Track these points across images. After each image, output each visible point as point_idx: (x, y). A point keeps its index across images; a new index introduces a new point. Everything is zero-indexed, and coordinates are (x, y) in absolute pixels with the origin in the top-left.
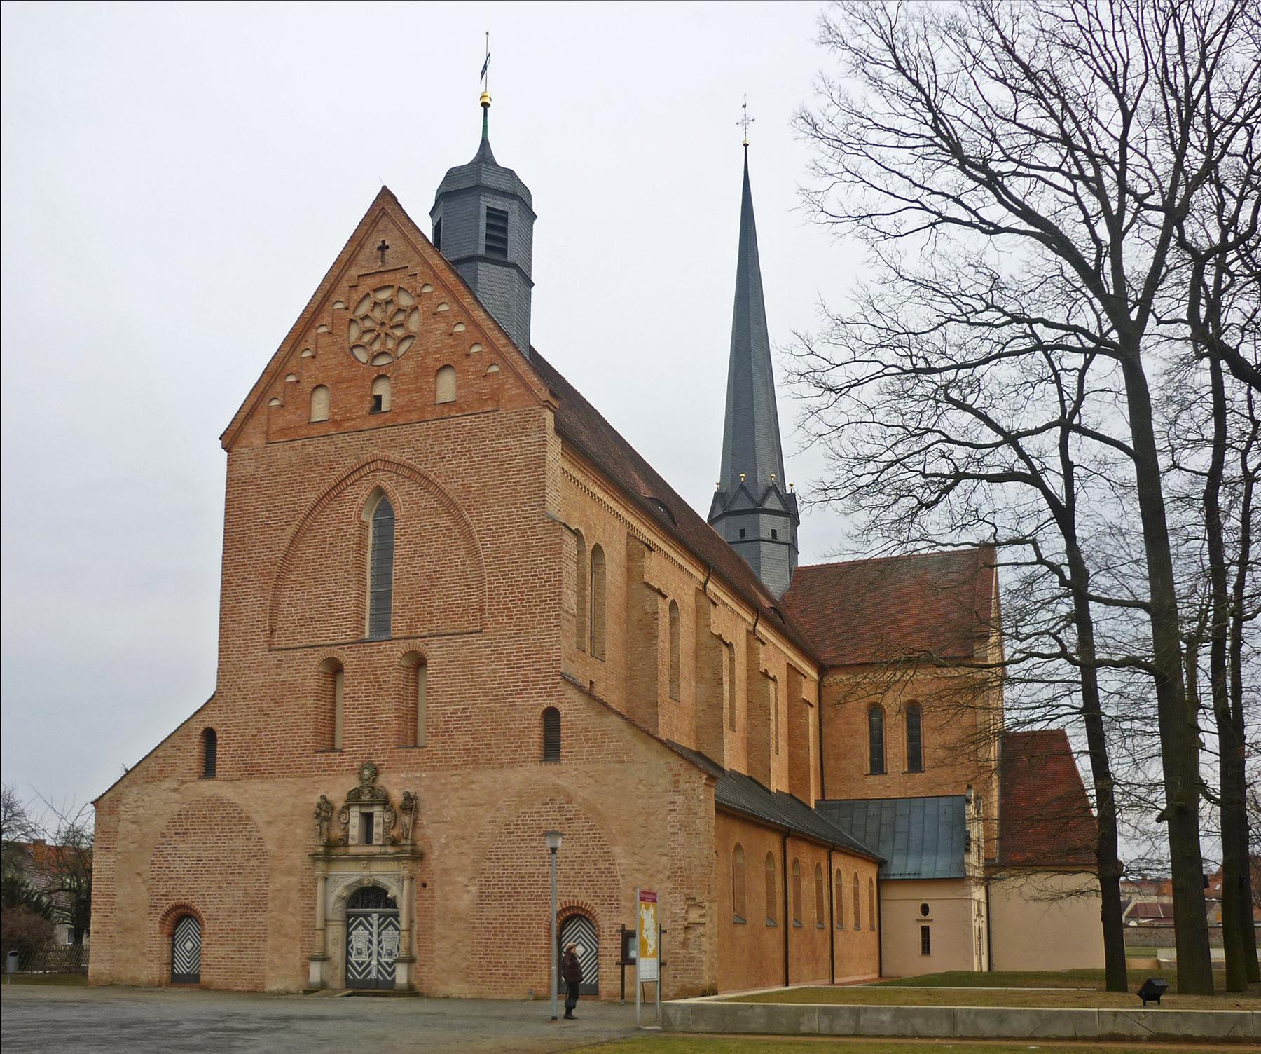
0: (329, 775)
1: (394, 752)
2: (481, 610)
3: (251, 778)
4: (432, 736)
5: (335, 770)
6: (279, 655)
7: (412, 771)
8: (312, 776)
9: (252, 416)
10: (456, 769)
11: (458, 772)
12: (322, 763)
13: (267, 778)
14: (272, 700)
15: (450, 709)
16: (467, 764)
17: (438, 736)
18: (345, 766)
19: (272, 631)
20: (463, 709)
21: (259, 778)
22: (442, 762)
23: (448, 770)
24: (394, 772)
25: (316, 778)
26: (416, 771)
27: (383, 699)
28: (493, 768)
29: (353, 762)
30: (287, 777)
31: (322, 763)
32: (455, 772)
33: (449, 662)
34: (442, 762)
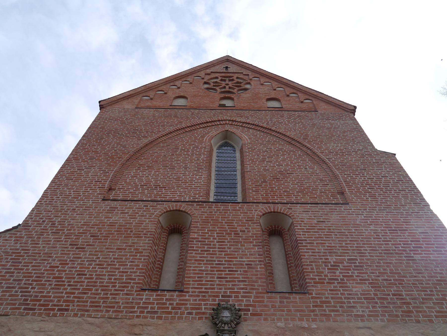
0: (160, 318)
1: (263, 297)
2: (342, 193)
3: (27, 314)
4: (315, 283)
5: (170, 313)
6: (113, 204)
7: (293, 319)
8: (131, 318)
9: (128, 99)
10: (362, 321)
11: (366, 324)
12: (150, 303)
13: (55, 315)
14: (91, 236)
15: (332, 259)
16: (377, 316)
17: (324, 283)
18: (187, 309)
19: (110, 189)
20: (348, 259)
21: (40, 315)
22: (337, 311)
23: (349, 321)
24: (266, 319)
25: (136, 321)
26: (301, 320)
27: (241, 245)
28: (418, 322)
29: (200, 304)
30: (90, 316)
31: (150, 303)
32: (361, 324)
33: (318, 221)
34: (337, 311)
